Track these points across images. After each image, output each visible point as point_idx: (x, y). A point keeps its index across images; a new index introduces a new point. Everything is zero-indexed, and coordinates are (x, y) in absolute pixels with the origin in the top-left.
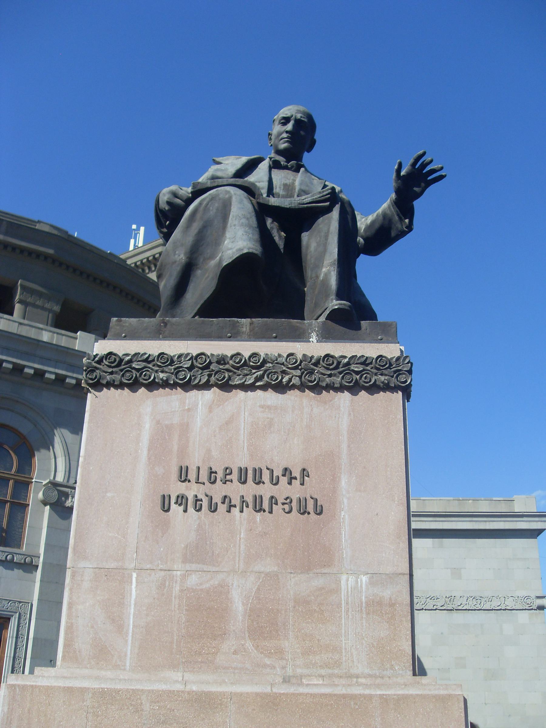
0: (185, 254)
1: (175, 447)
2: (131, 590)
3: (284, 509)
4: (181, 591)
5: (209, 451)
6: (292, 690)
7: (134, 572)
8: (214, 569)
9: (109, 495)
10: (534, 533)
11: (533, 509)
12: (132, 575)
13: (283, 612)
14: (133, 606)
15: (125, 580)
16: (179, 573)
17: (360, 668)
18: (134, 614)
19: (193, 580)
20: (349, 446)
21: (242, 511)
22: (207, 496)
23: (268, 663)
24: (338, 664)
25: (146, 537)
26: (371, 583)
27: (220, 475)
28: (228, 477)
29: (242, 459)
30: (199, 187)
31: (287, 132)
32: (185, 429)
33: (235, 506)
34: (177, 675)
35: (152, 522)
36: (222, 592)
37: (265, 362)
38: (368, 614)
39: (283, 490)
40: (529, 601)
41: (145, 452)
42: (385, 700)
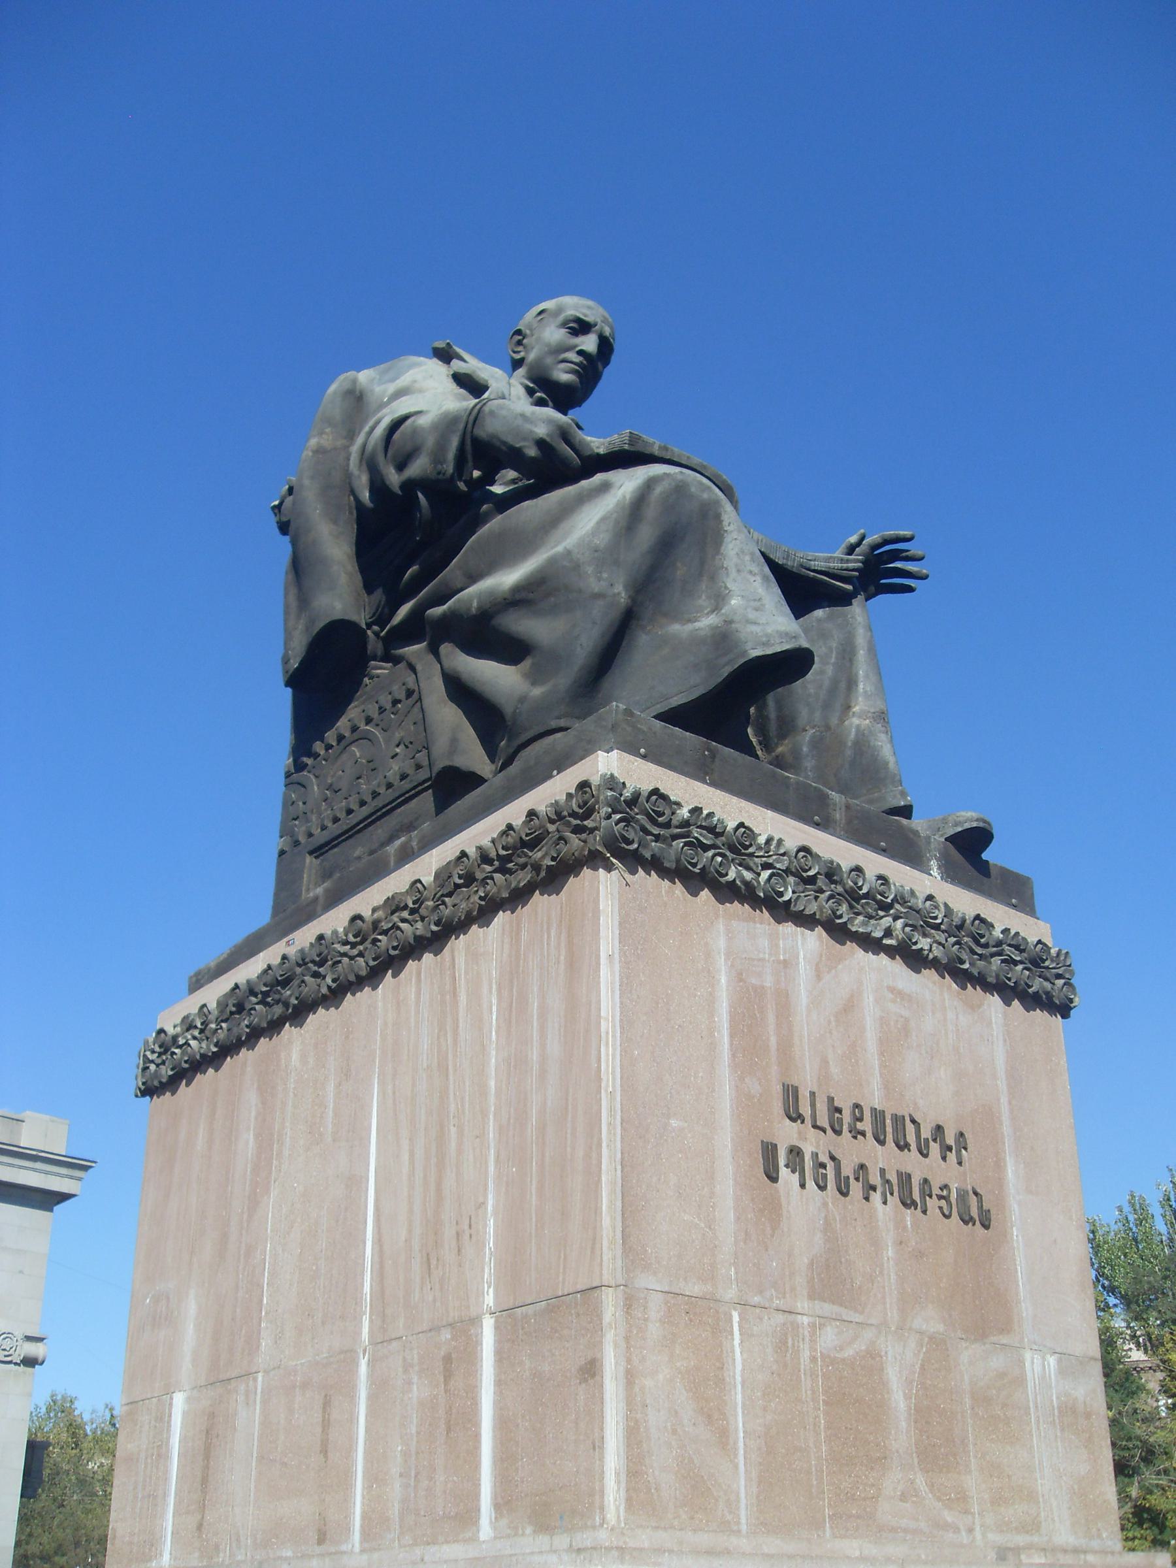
0: (626, 587)
1: (773, 1040)
2: (733, 1351)
3: (941, 1208)
4: (813, 1359)
5: (825, 1062)
7: (735, 1310)
8: (858, 1318)
9: (674, 1123)
10: (47, 1200)
11: (59, 1146)
12: (731, 1315)
13: (959, 1417)
14: (739, 1387)
15: (720, 1329)
16: (805, 1320)
18: (744, 1405)
19: (829, 1337)
20: (1010, 1103)
21: (885, 1203)
22: (833, 1158)
23: (949, 1519)
25: (746, 1233)
26: (1062, 1372)
27: (847, 1117)
28: (859, 1126)
30: (639, 448)
31: (581, 353)
33: (874, 1188)
35: (753, 1200)
37: (895, 900)
38: (1062, 1430)
40: (7, 1344)
41: (726, 1039)
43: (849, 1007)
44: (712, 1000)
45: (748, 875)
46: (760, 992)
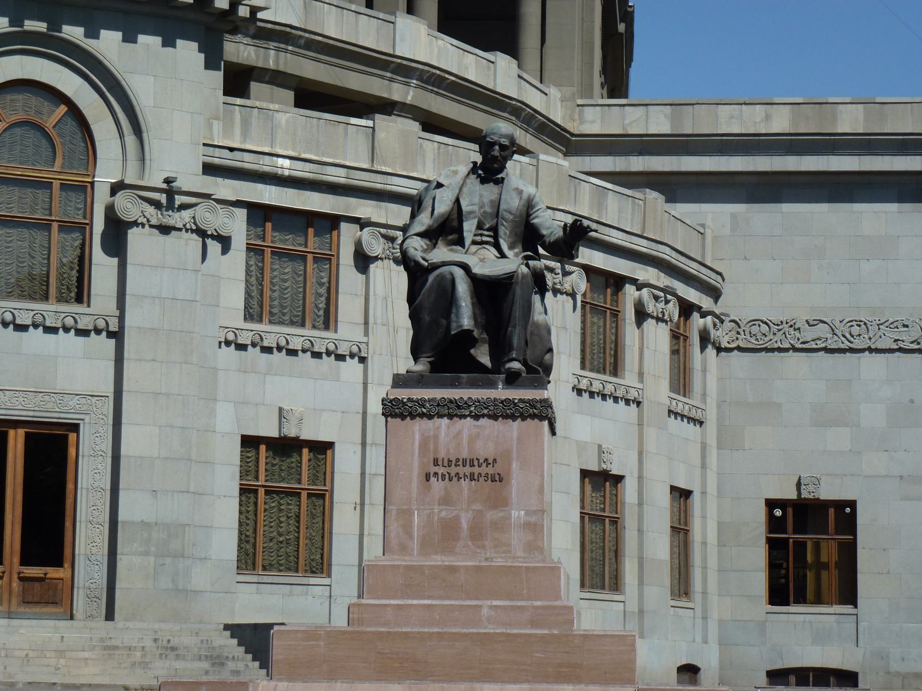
6: (488, 564)
17: (520, 554)
19: (443, 514)
24: (510, 552)
26: (526, 514)
29: (465, 454)
32: (436, 437)
34: (438, 557)
36: (457, 518)
39: (484, 470)
42: (527, 568)
43: (459, 433)
44: (413, 442)
45: (424, 410)
46: (429, 437)
